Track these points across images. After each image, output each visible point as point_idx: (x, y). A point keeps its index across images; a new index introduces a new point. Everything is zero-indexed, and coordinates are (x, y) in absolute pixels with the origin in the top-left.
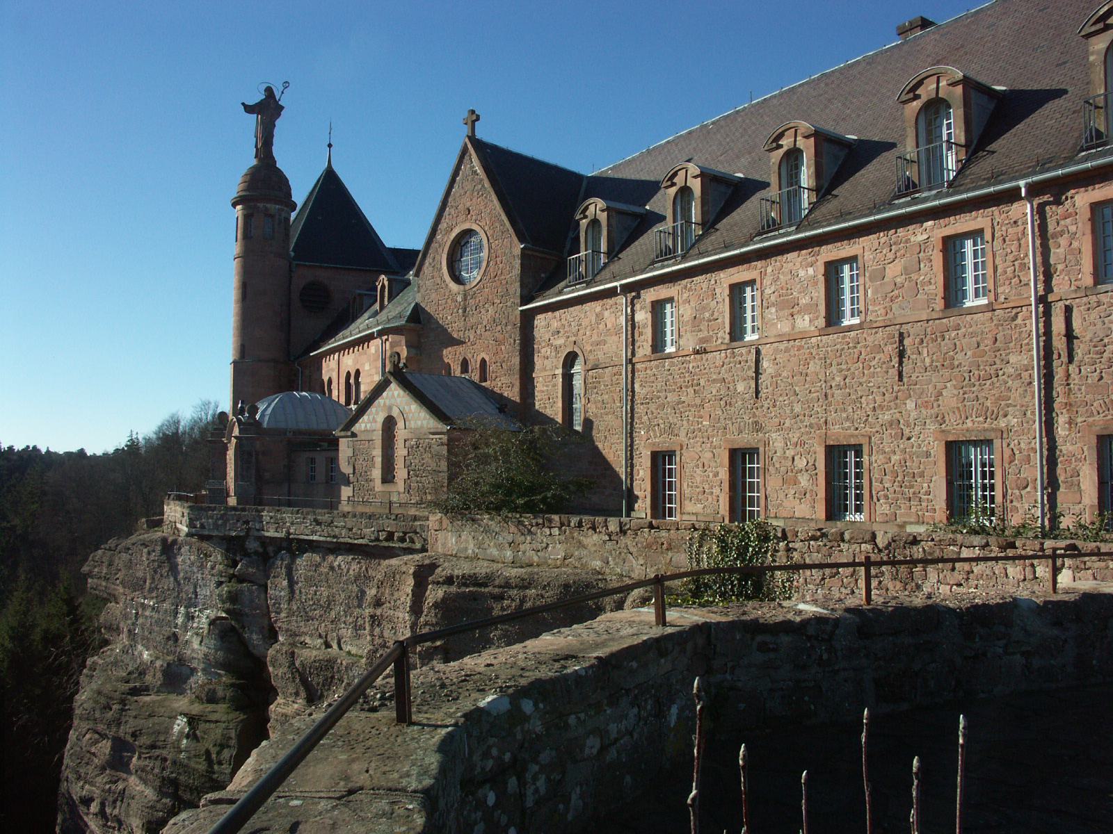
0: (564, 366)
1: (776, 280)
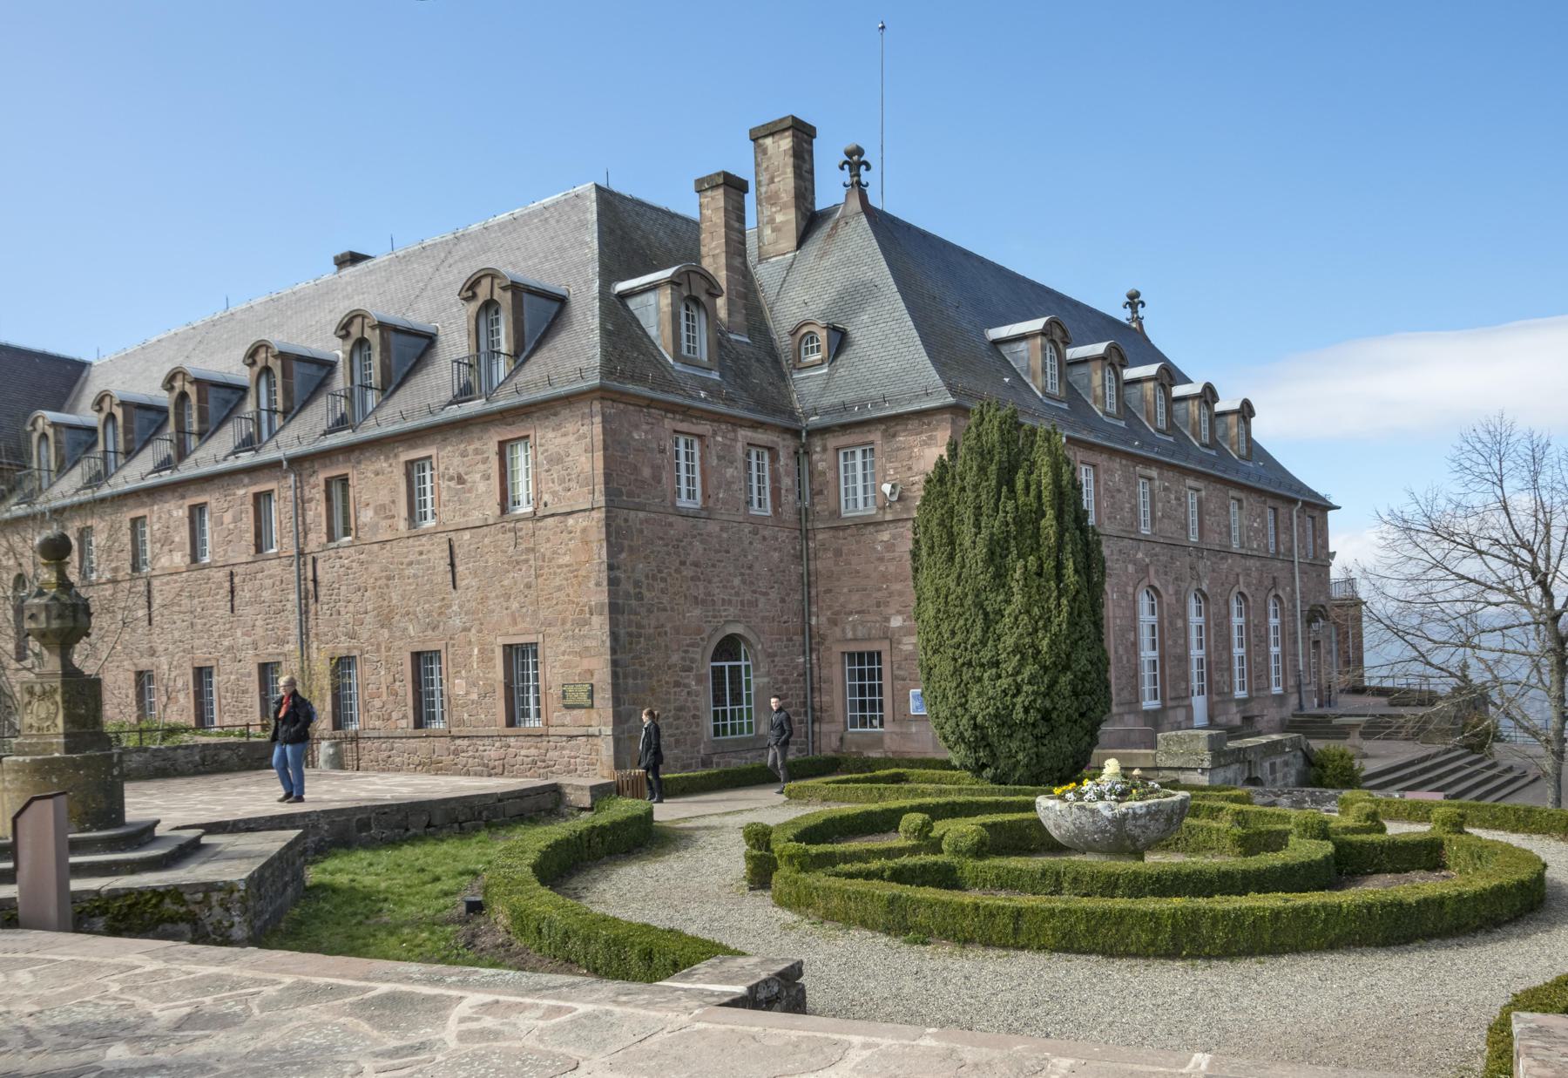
1: (160, 518)
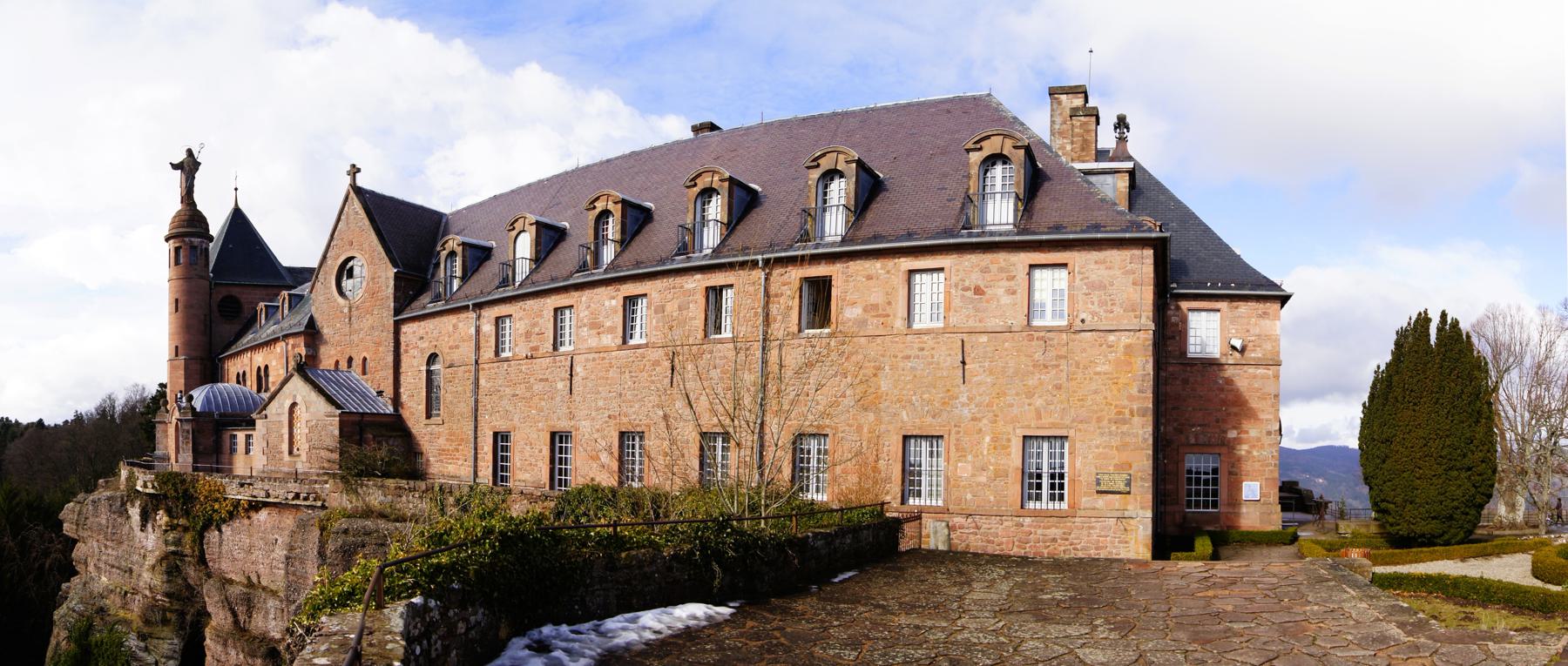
0: (428, 364)
